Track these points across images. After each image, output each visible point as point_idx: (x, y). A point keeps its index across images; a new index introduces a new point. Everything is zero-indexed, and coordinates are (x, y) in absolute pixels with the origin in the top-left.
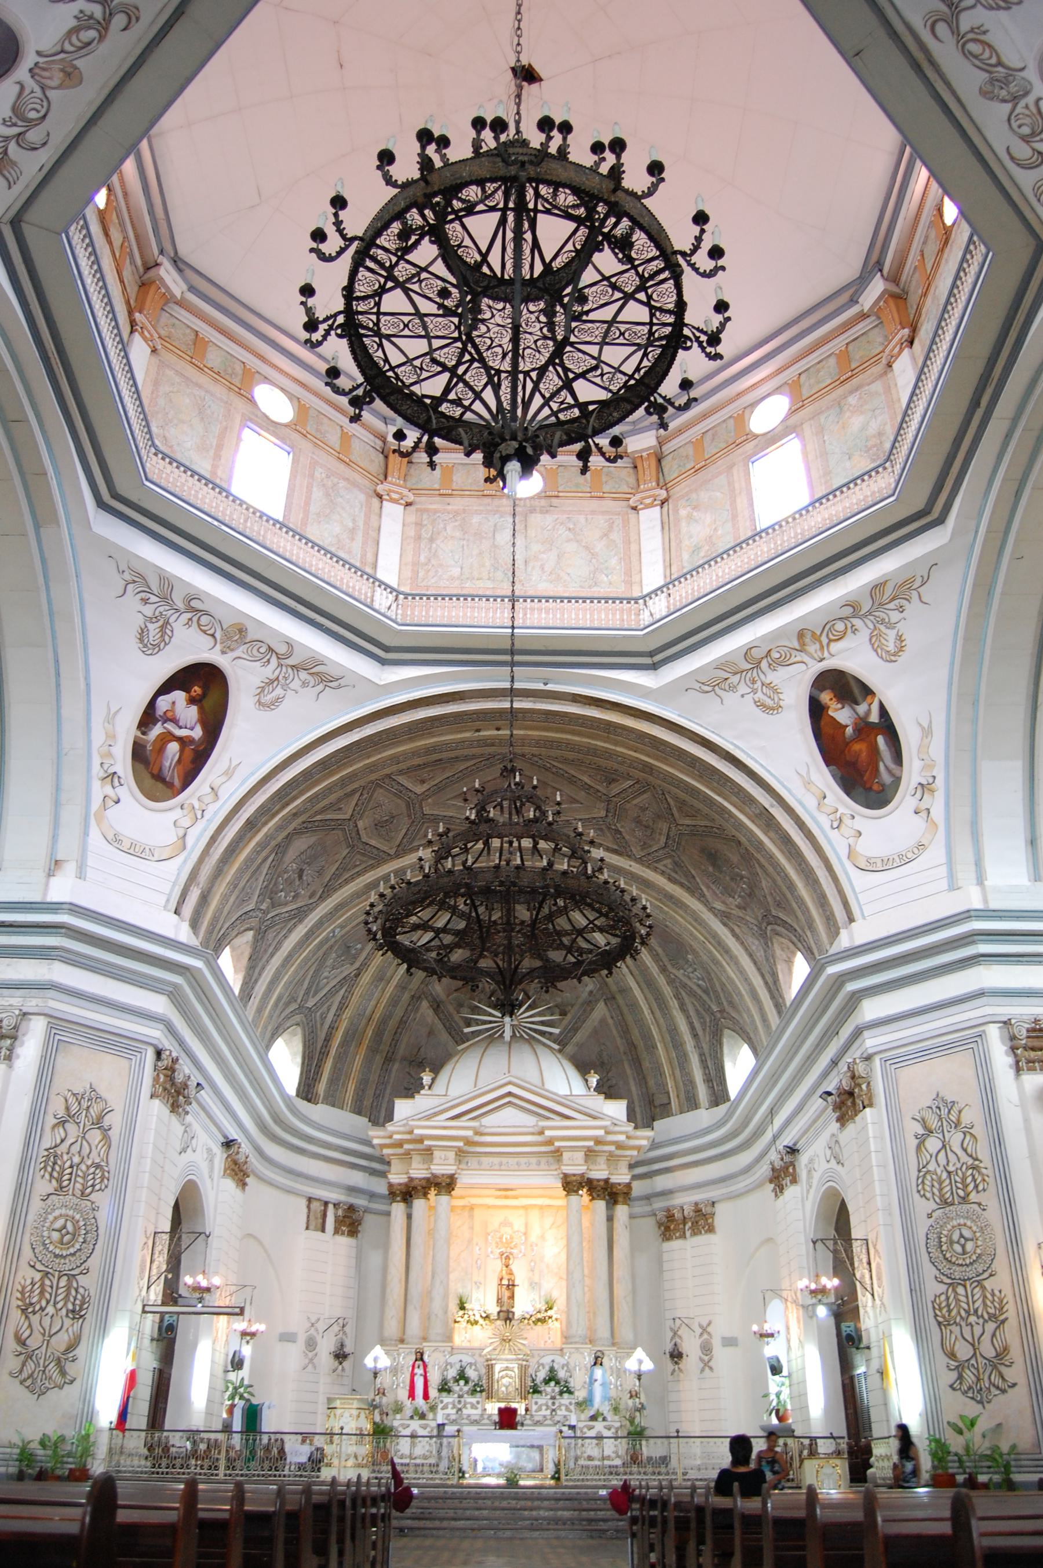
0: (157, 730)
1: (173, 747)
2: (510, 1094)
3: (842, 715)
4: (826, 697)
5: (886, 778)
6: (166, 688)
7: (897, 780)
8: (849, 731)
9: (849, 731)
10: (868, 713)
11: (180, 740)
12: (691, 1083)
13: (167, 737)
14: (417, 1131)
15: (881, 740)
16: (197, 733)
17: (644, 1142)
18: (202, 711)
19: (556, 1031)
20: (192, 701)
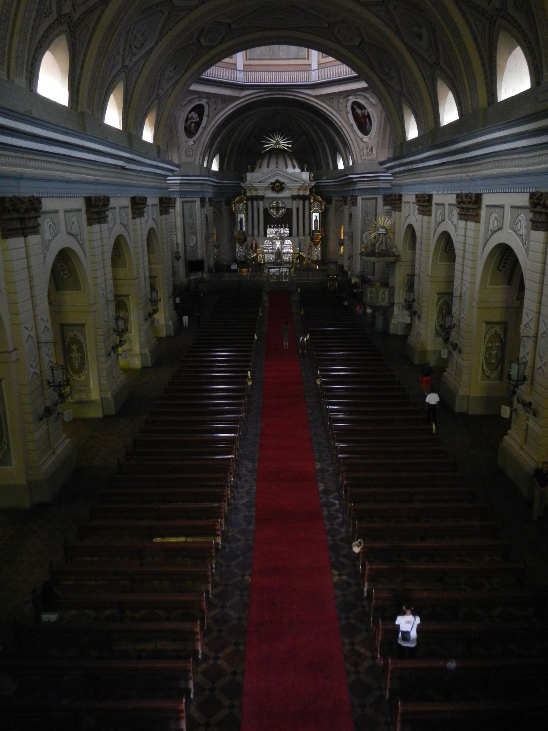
0: (189, 122)
1: (193, 125)
2: (277, 173)
3: (359, 111)
4: (355, 107)
5: (368, 129)
6: (190, 112)
7: (370, 130)
8: (360, 115)
9: (360, 115)
10: (365, 113)
11: (195, 123)
12: (328, 163)
13: (192, 122)
14: (254, 185)
15: (367, 120)
16: (198, 119)
17: (313, 185)
18: (198, 115)
19: (290, 146)
20: (196, 113)
